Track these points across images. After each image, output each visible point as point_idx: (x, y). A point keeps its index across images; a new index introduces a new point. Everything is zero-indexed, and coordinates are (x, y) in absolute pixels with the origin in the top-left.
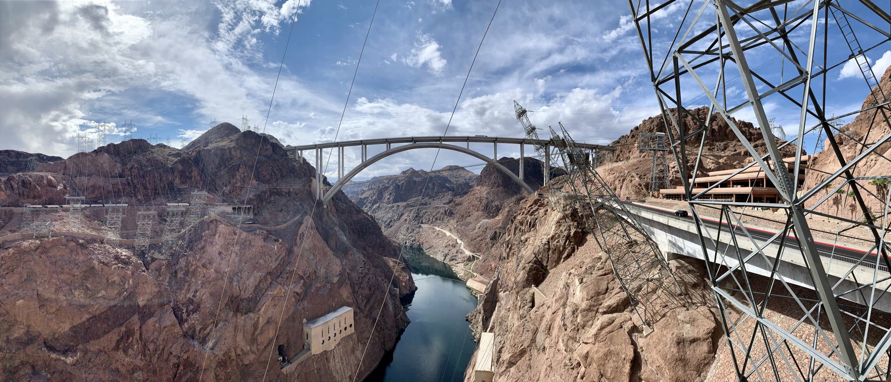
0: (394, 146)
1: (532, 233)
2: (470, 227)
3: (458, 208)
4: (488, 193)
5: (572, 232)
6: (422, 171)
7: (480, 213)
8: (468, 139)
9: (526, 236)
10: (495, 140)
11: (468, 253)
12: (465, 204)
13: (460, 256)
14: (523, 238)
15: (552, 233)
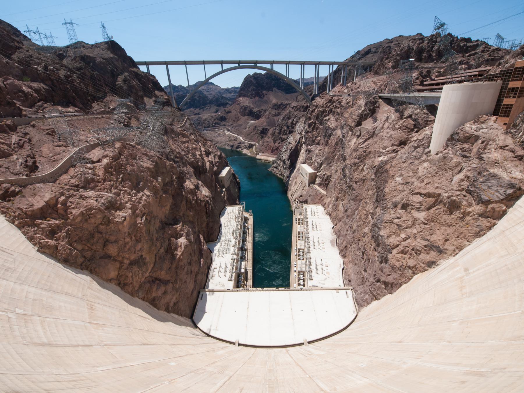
0: (226, 67)
1: (331, 116)
2: (242, 127)
3: (229, 114)
4: (249, 103)
5: (372, 108)
6: (180, 86)
7: (246, 117)
8: (272, 63)
9: (327, 118)
10: (288, 63)
11: (247, 142)
12: (234, 112)
13: (243, 145)
14: (325, 118)
15: (363, 109)
